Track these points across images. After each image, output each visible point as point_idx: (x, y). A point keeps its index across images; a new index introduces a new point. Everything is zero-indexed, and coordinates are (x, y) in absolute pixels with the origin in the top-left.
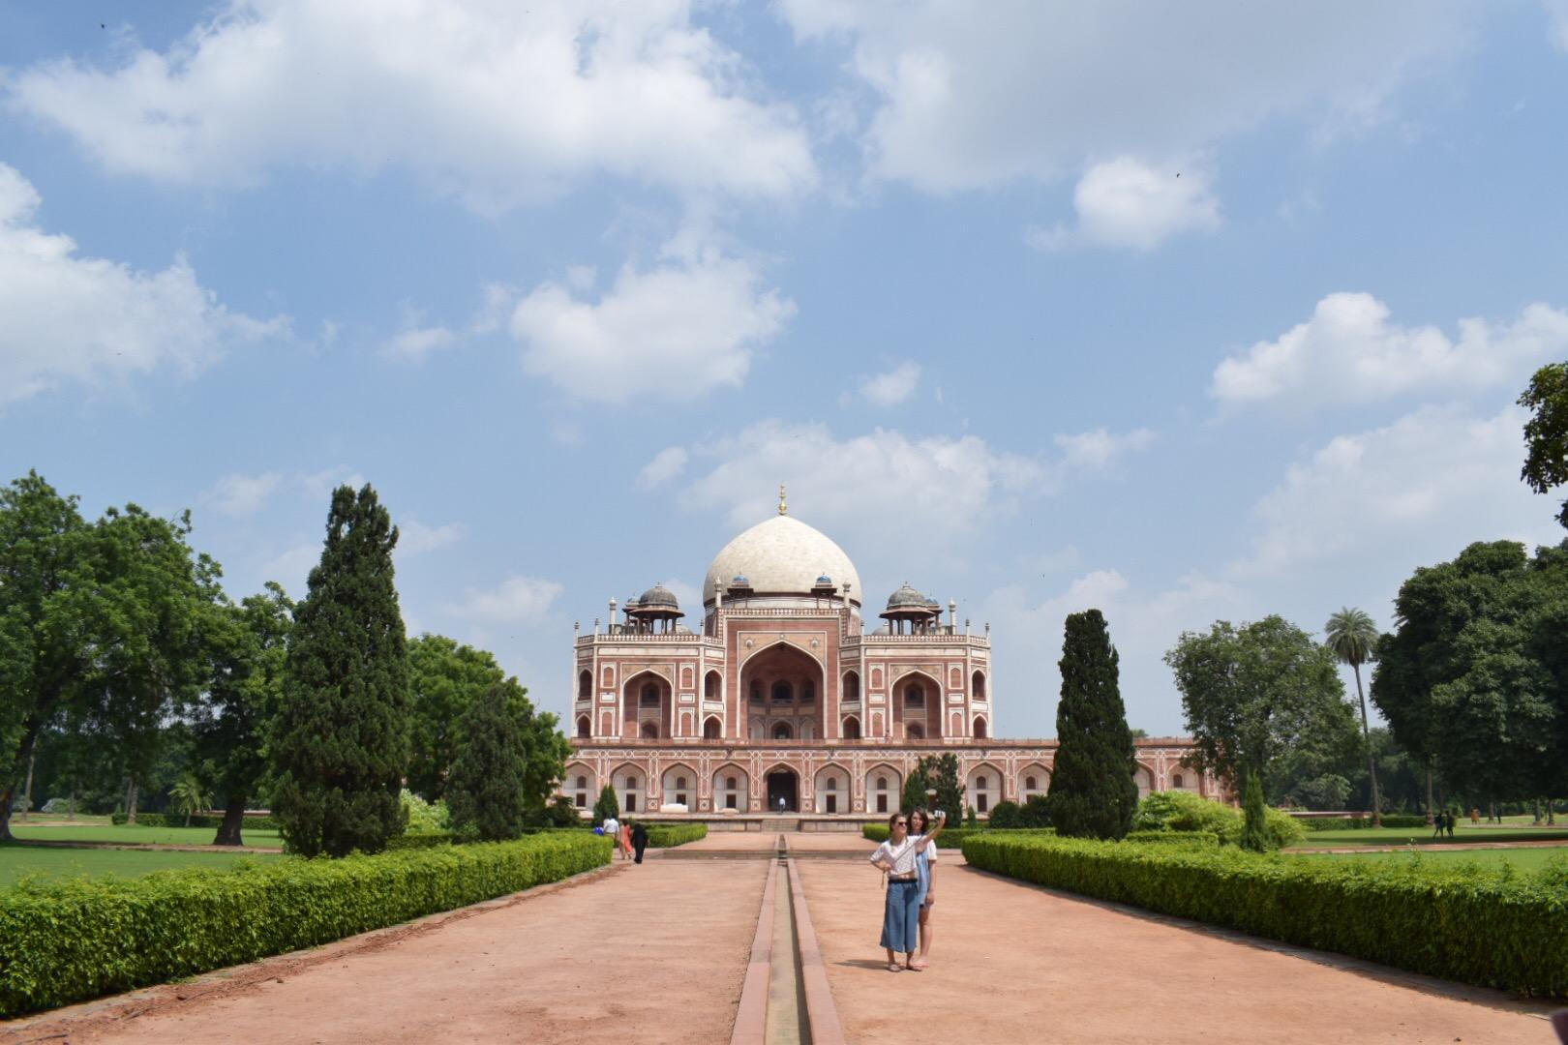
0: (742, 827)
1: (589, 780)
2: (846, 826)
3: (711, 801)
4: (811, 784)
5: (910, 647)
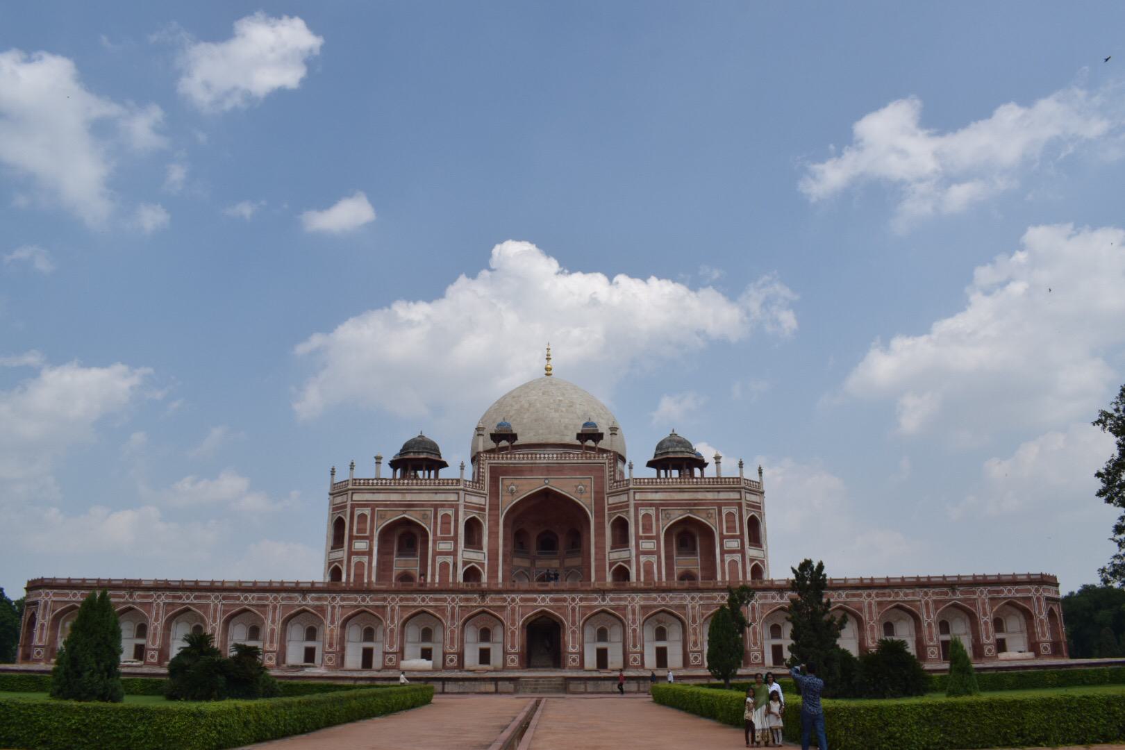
0: (492, 687)
1: (319, 635)
3: (461, 656)
4: (578, 635)
5: (682, 490)
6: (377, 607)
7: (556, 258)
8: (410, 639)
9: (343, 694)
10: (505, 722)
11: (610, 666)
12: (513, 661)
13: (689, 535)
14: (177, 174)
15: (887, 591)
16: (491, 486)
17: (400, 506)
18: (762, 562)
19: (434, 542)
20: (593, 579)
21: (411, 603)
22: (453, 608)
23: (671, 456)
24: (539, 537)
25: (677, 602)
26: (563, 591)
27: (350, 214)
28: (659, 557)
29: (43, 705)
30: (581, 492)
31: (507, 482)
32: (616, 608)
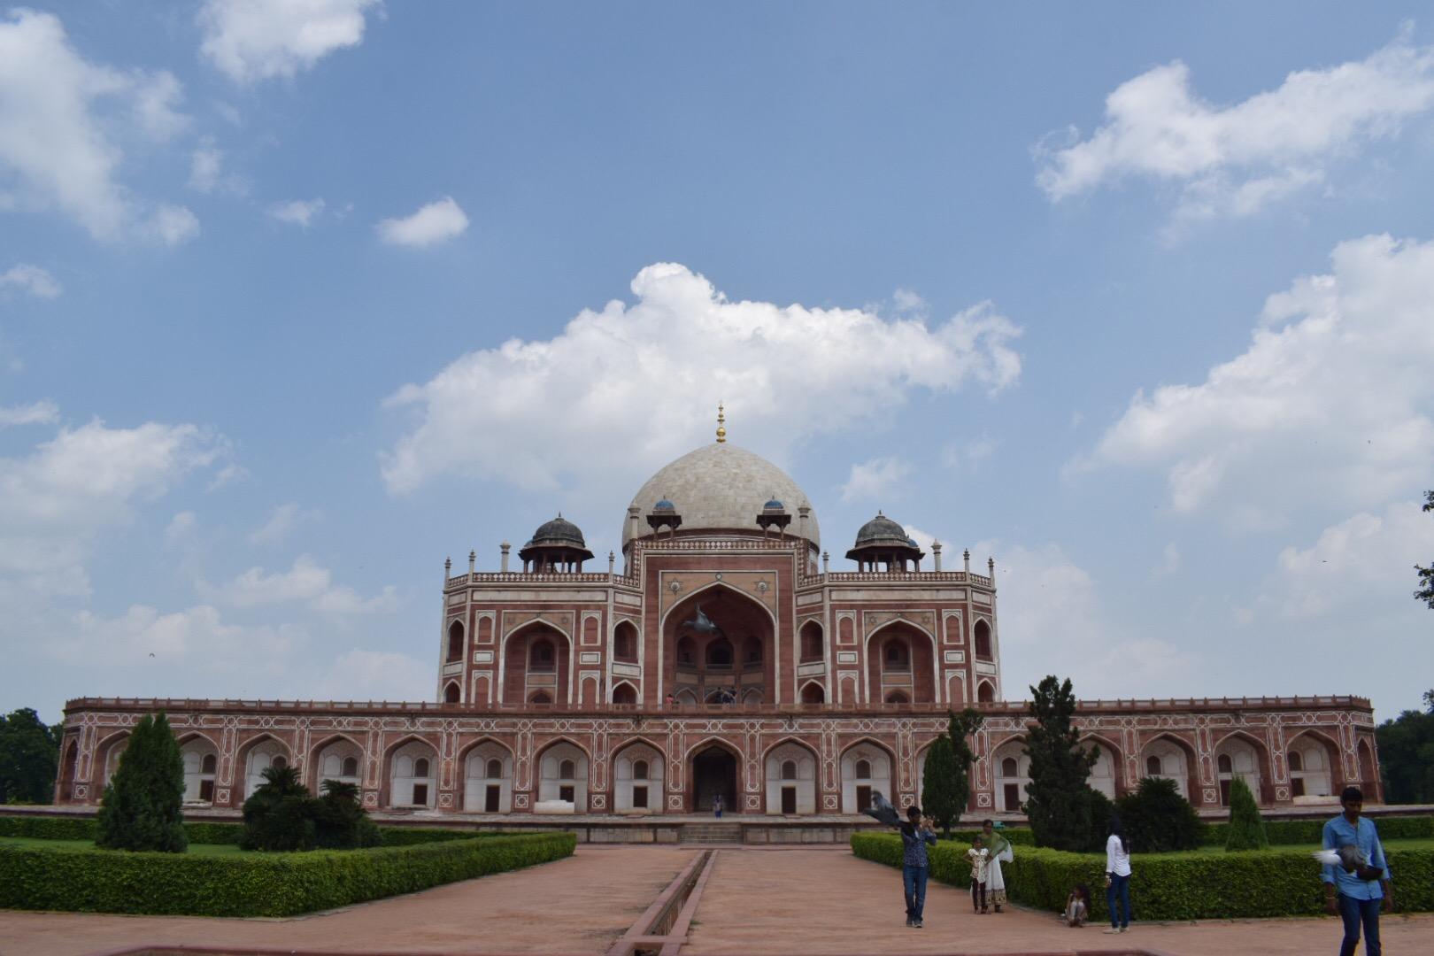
0: (649, 836)
2: (814, 835)
3: (610, 796)
5: (890, 588)
6: (505, 734)
7: (707, 277)
8: (546, 775)
9: (463, 843)
10: (665, 880)
11: (798, 810)
12: (676, 802)
13: (900, 645)
14: (206, 164)
15: (1152, 717)
16: (648, 583)
17: (534, 607)
18: (993, 679)
19: (577, 653)
20: (777, 700)
21: (548, 730)
22: (600, 736)
23: (877, 544)
24: (709, 647)
25: (884, 730)
26: (739, 715)
27: (436, 222)
28: (862, 673)
29: (87, 856)
30: (763, 590)
31: (669, 577)
32: (807, 737)
